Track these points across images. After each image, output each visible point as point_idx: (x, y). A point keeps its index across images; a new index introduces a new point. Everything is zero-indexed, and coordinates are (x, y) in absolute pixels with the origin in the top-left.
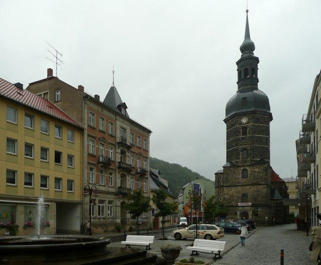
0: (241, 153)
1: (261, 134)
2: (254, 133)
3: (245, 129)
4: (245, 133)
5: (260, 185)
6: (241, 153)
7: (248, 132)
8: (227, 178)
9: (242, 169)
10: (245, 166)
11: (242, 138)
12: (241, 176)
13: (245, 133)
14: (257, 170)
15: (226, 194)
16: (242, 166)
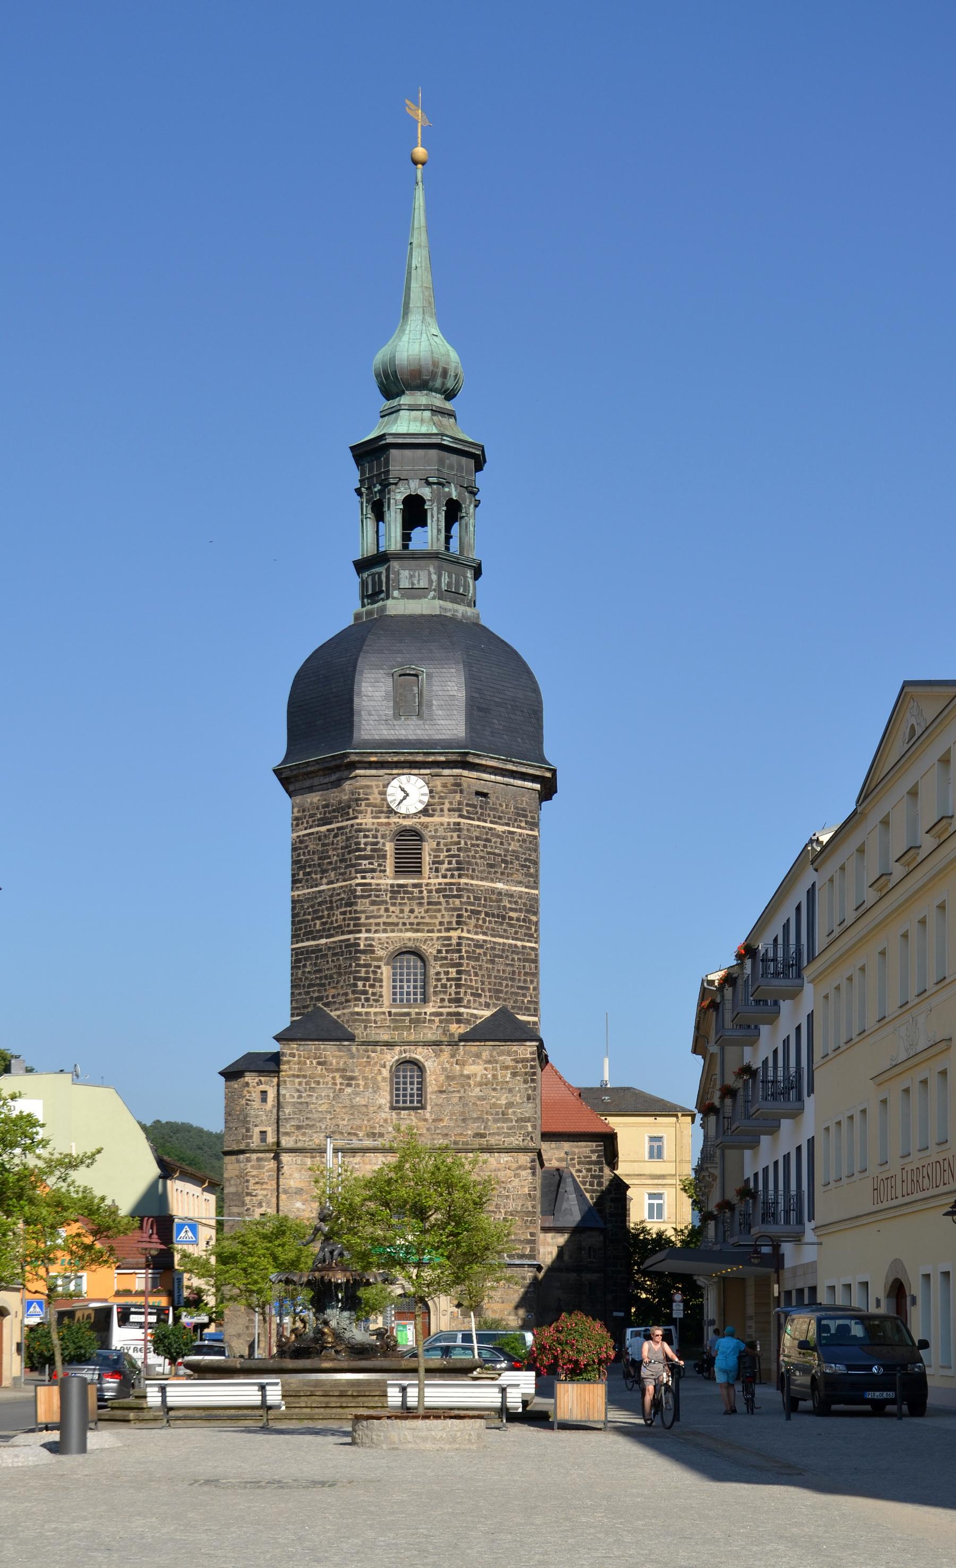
0: (386, 972)
1: (504, 876)
2: (460, 869)
3: (409, 840)
4: (409, 862)
5: (489, 1150)
6: (386, 972)
7: (427, 859)
8: (302, 1106)
9: (391, 1057)
10: (409, 1043)
11: (396, 891)
12: (384, 1098)
13: (409, 862)
14: (476, 1069)
15: (299, 1191)
16: (389, 1045)
